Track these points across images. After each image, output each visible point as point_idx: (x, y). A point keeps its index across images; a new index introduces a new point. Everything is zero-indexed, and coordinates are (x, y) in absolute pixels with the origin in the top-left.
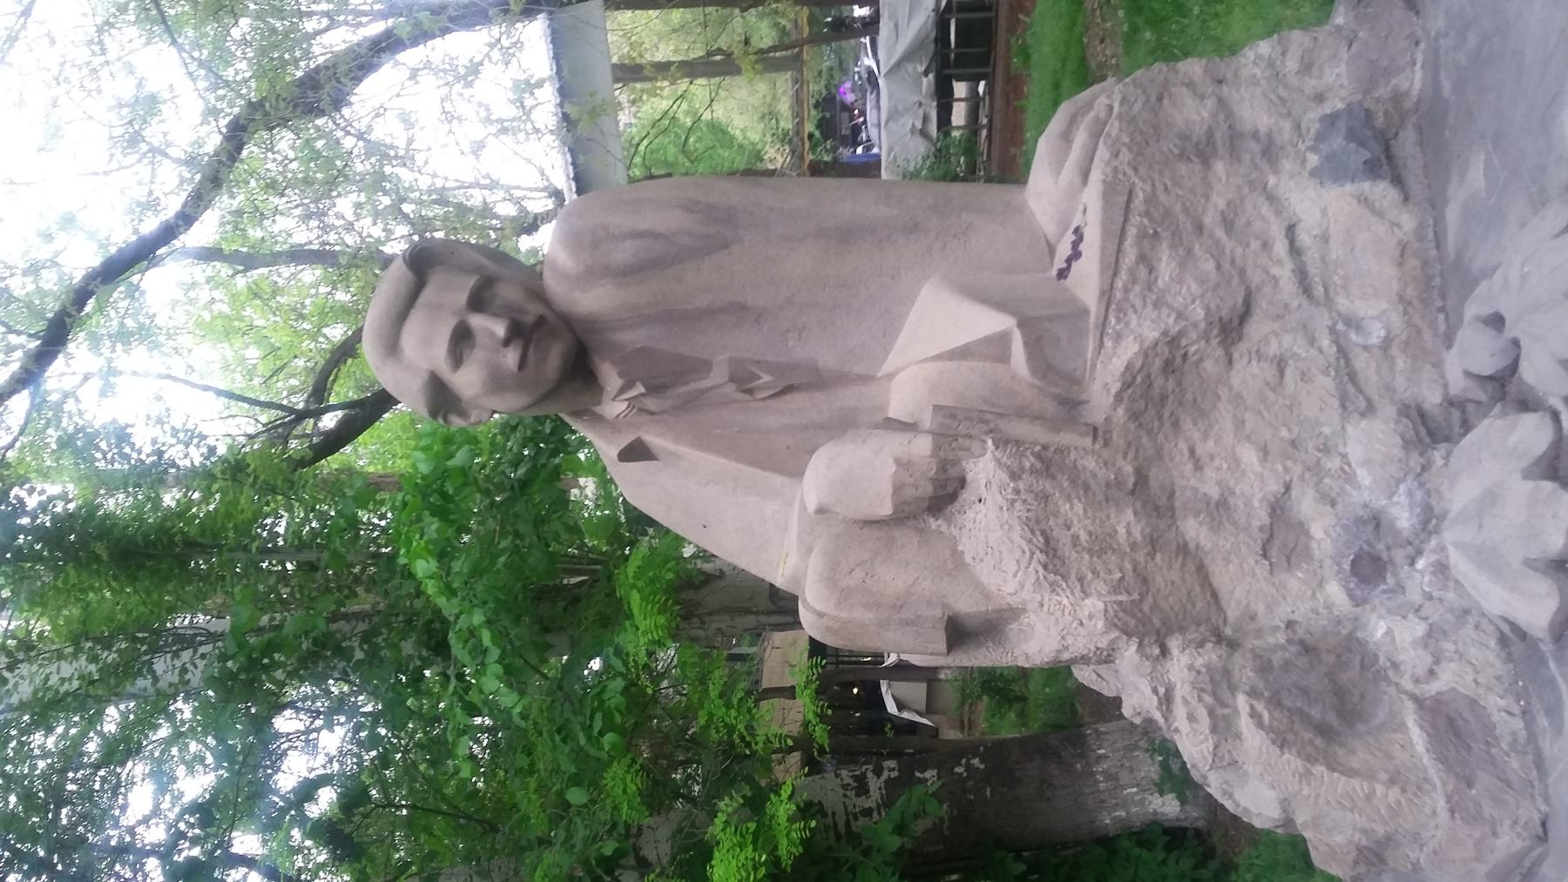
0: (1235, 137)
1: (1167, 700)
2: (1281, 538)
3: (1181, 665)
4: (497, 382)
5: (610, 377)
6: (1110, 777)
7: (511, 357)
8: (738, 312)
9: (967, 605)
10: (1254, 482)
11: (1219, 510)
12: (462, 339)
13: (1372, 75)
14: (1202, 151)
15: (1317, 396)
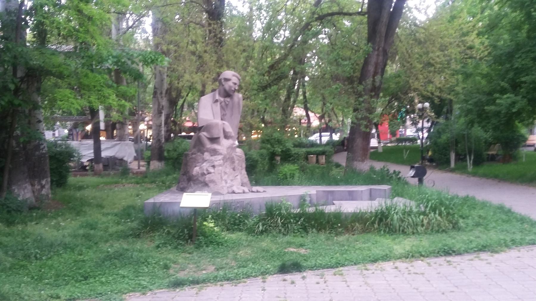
0: (242, 169)
1: (220, 160)
2: (225, 173)
3: (222, 161)
4: (230, 87)
5: (228, 99)
6: (26, 187)
7: (233, 89)
8: (232, 115)
9: (221, 139)
10: (227, 170)
11: (226, 167)
12: (235, 84)
13: (245, 183)
14: (241, 167)
15: (231, 178)
